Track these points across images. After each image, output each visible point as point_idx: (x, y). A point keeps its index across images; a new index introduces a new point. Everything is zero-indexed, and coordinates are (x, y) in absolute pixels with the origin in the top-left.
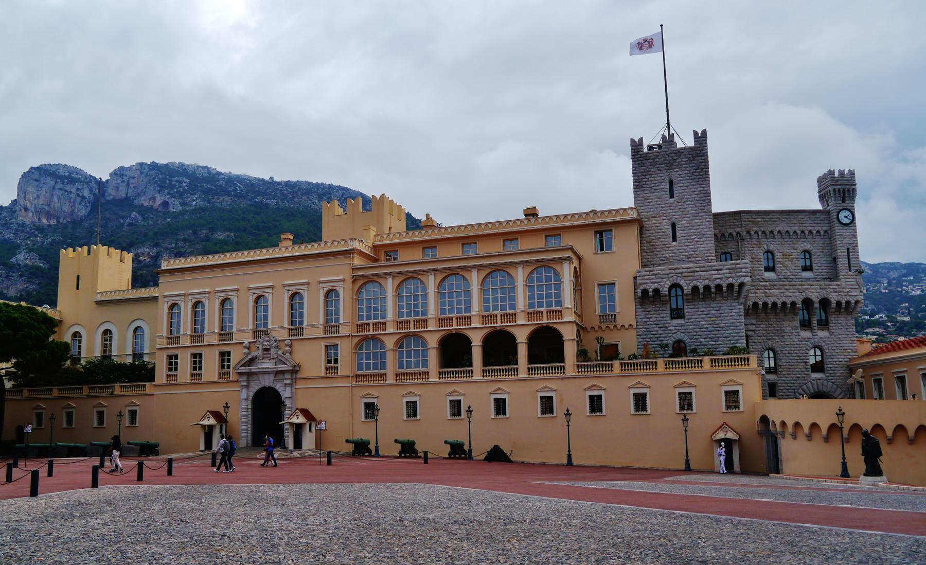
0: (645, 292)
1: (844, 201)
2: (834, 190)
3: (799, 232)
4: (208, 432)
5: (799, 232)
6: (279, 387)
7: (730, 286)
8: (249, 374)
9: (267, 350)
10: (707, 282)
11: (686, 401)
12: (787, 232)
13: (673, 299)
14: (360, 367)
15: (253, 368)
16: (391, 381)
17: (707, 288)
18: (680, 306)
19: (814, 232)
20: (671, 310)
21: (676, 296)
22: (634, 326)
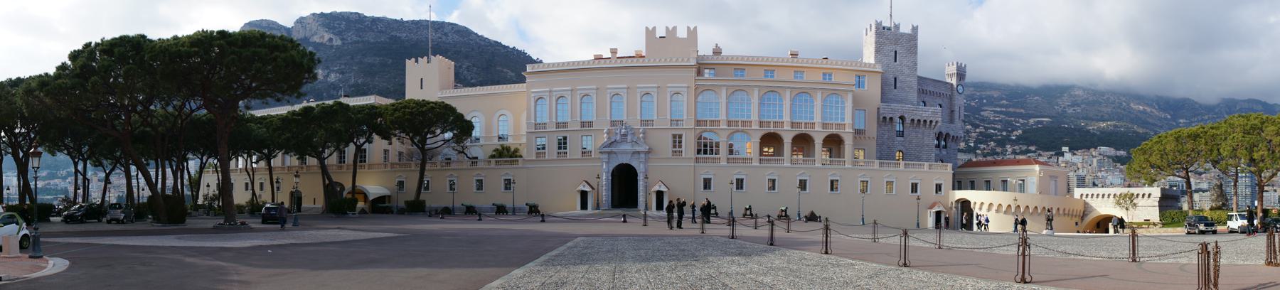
4: (584, 194)
6: (634, 164)
8: (609, 153)
9: (625, 135)
11: (914, 188)
14: (699, 152)
15: (613, 149)
16: (724, 163)
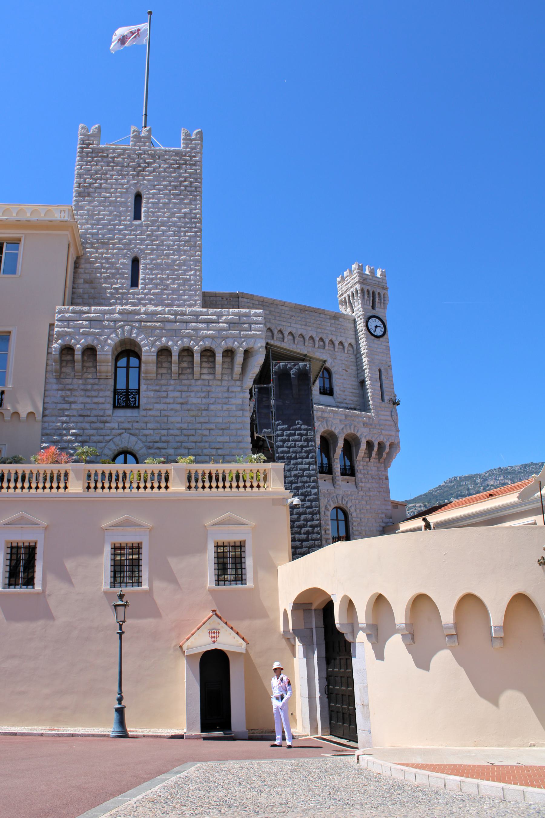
0: (68, 350)
1: (373, 307)
2: (362, 290)
3: (317, 339)
5: (317, 339)
7: (229, 353)
10: (187, 342)
12: (301, 335)
13: (122, 373)
17: (187, 352)
18: (133, 385)
19: (337, 343)
20: (115, 391)
21: (128, 367)
22: (39, 417)
